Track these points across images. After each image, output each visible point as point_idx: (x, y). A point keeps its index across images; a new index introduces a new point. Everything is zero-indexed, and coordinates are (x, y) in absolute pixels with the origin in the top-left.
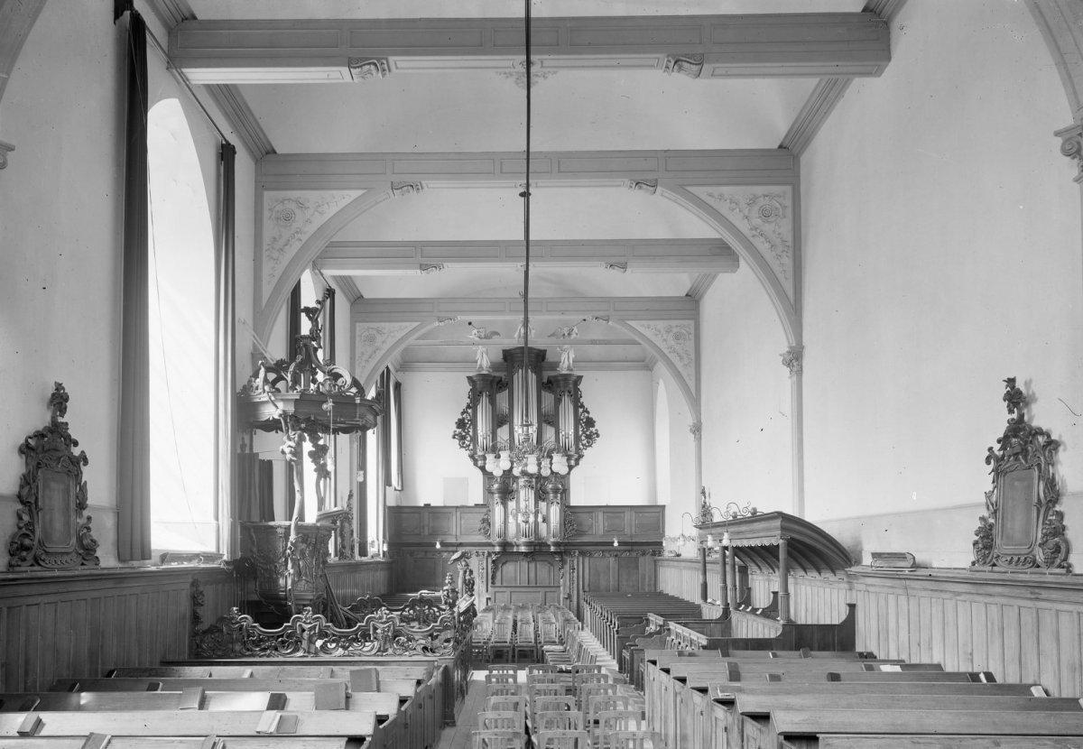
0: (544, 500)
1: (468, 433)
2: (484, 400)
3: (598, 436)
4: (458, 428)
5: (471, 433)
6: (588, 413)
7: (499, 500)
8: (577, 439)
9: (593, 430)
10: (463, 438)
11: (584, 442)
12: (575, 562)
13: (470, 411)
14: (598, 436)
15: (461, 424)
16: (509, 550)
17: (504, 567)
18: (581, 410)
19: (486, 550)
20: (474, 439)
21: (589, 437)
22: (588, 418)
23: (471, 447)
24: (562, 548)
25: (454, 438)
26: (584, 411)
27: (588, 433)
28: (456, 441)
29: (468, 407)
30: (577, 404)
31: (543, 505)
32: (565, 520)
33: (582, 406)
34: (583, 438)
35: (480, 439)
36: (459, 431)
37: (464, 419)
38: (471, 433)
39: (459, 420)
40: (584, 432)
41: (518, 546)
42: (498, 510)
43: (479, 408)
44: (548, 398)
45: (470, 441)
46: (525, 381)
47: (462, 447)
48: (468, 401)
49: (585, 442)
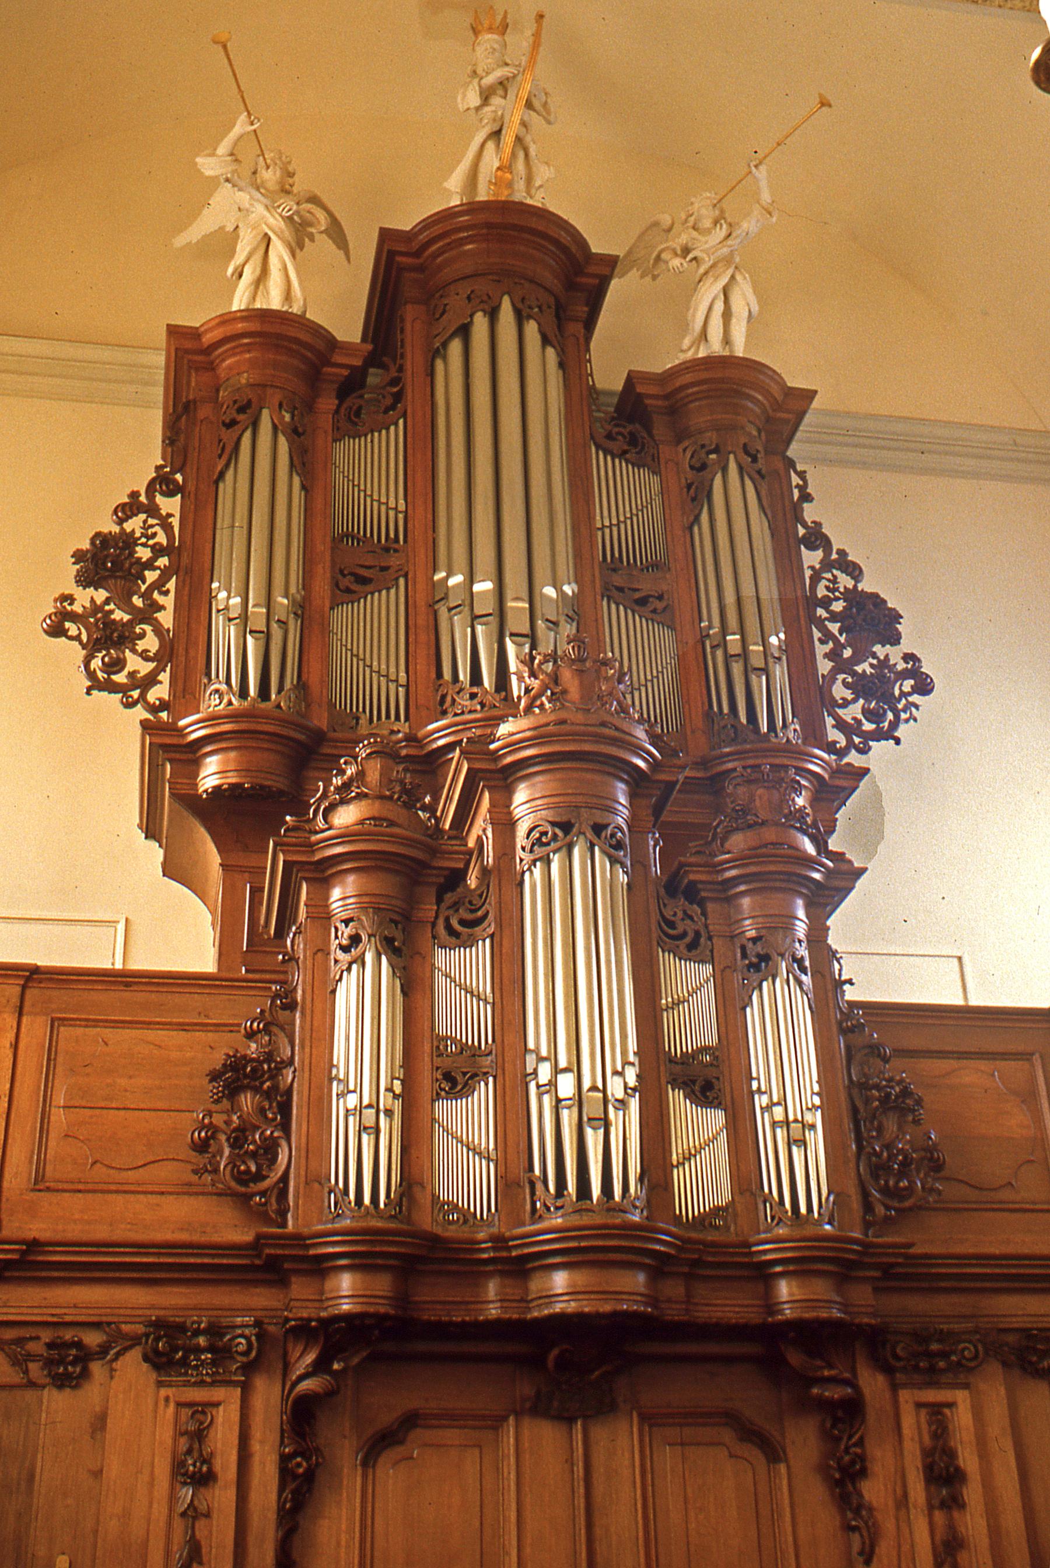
0: (692, 948)
1: (148, 614)
2: (266, 448)
3: (924, 687)
4: (85, 580)
5: (166, 618)
7: (366, 925)
8: (812, 699)
9: (894, 654)
10: (109, 638)
11: (848, 714)
12: (962, 1417)
13: (170, 505)
14: (924, 687)
15: (106, 561)
16: (437, 1301)
17: (390, 1476)
18: (811, 558)
19: (244, 1306)
20: (186, 654)
21: (876, 689)
22: (853, 596)
23: (160, 692)
24: (862, 1296)
25: (56, 630)
26: (827, 564)
27: (864, 667)
28: (70, 652)
29: (162, 483)
30: (790, 528)
31: (689, 981)
32: (859, 1087)
33: (817, 538)
35: (225, 635)
36: (84, 598)
37: (128, 541)
38: (166, 618)
39: (102, 541)
40: (841, 666)
41: (521, 1267)
42: (357, 1011)
43: (232, 489)
44: (628, 496)
45: (162, 658)
47: (96, 685)
49: (853, 712)
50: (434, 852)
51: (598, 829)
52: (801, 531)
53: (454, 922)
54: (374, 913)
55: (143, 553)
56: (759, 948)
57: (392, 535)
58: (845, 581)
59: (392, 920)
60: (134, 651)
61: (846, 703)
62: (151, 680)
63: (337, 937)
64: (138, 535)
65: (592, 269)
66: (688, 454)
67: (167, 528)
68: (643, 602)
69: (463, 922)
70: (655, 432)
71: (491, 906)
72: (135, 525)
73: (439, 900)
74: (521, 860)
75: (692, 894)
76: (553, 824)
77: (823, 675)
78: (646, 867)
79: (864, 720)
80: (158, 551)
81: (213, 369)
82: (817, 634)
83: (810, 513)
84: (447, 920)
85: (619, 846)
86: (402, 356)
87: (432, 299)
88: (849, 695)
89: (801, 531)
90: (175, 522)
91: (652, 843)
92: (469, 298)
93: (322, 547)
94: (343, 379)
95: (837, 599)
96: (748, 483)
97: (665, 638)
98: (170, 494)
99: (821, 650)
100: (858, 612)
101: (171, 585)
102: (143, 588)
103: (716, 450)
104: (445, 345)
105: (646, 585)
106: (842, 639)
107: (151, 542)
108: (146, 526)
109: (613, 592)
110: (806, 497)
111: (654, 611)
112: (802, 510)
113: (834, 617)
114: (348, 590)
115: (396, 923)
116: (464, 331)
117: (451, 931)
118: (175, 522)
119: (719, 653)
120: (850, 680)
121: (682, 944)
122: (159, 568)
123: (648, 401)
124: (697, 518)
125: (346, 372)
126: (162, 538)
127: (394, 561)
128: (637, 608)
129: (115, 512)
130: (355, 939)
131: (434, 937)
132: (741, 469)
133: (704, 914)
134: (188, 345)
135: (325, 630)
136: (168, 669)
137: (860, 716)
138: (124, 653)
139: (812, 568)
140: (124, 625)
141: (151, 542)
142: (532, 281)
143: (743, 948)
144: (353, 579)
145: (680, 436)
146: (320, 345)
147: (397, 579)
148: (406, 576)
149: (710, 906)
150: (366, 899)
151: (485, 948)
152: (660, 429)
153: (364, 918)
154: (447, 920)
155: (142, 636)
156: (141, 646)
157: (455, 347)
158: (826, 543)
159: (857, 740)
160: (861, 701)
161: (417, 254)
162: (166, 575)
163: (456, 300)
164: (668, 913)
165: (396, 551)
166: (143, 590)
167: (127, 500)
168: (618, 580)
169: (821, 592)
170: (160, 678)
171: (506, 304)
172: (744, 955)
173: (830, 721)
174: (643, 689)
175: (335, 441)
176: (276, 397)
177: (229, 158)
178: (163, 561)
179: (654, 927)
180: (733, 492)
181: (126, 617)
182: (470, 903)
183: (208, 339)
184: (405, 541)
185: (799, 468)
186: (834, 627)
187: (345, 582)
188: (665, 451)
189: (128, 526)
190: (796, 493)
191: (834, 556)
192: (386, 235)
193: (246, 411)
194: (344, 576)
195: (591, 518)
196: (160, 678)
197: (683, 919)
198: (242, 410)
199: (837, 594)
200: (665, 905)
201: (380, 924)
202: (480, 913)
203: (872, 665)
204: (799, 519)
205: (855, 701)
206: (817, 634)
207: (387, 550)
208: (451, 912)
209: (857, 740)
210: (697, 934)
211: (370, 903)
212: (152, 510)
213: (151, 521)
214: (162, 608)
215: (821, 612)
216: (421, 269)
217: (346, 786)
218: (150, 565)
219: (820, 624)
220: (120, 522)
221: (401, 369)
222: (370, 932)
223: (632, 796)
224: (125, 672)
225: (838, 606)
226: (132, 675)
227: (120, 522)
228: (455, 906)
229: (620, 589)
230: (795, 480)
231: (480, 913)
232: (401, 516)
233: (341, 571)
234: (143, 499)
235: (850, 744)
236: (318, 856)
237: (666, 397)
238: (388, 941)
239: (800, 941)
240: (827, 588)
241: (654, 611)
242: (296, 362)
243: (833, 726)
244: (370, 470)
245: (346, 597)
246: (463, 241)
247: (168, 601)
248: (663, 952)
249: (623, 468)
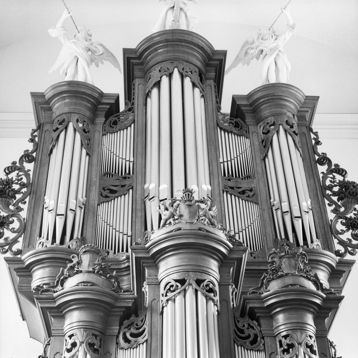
6: (342, 172)
13: (29, 166)
18: (322, 169)
26: (330, 171)
29: (27, 157)
33: (324, 160)
34: (339, 227)
37: (9, 183)
38: (24, 214)
40: (339, 216)
44: (235, 149)
46: (176, 106)
48: (30, 147)
49: (347, 236)
50: (117, 299)
51: (199, 282)
52: (317, 157)
53: (128, 335)
54: (85, 331)
55: (16, 187)
56: (288, 341)
57: (127, 172)
58: (339, 178)
59: (93, 334)
60: (8, 228)
61: (343, 232)
62: (15, 241)
63: (66, 345)
64: (14, 179)
65: (216, 57)
66: (262, 128)
67: (27, 175)
68: (243, 192)
69: (132, 335)
70: (246, 121)
71: (146, 326)
72: (13, 175)
73: (121, 324)
74: (162, 301)
75: (252, 315)
76: (176, 281)
77: (331, 220)
78: (228, 302)
79: (352, 240)
80: (23, 185)
81: (51, 110)
82: (327, 202)
83: (320, 149)
84: (124, 334)
85: (211, 290)
86: (133, 99)
87: (145, 75)
88: (344, 228)
89: (317, 157)
90: (31, 173)
91: (231, 290)
92: (160, 71)
93: (95, 178)
94: (107, 110)
95: (336, 186)
96: (290, 138)
97: (254, 209)
98: (30, 162)
99: (329, 209)
100: (346, 190)
101: (27, 200)
102: (15, 201)
103: (274, 124)
104: (150, 92)
105: (245, 185)
106: (339, 203)
107: (19, 182)
108: (18, 175)
109: (229, 190)
110: (318, 143)
111: (248, 196)
112: (317, 148)
113: (335, 194)
114: (107, 197)
115: (96, 336)
116: (158, 84)
117: (127, 340)
118: (31, 173)
119: (279, 212)
120: (344, 221)
121: (248, 341)
122: (22, 193)
123: (243, 108)
124: (266, 156)
125: (108, 107)
126: (25, 180)
127: (127, 182)
128: (240, 195)
129: (5, 170)
130: (74, 345)
131: (117, 343)
132: (286, 131)
133: (259, 325)
134: (40, 100)
135: (96, 215)
136: (23, 236)
137: (350, 238)
138: (3, 230)
139: (323, 173)
140: (4, 218)
141: (19, 182)
142: (187, 62)
143: (280, 342)
144: (108, 191)
145: (258, 121)
146: (96, 95)
147: (129, 190)
148: (132, 188)
149: (262, 321)
150: (81, 324)
151: (143, 348)
152: (249, 120)
153: (78, 334)
154: (124, 334)
155: (12, 222)
156: (11, 226)
157: (155, 91)
158: (329, 162)
159: (350, 249)
160: (351, 231)
161: (140, 57)
162: (25, 195)
163: (155, 74)
164: (240, 325)
165: (129, 178)
166: (14, 202)
167: (10, 165)
168: (231, 184)
169: (328, 183)
170: (18, 240)
171: (176, 71)
172: (281, 346)
173: (336, 241)
174: (244, 232)
175: (103, 135)
176: (75, 117)
177: (62, 29)
178: (24, 190)
179: (232, 332)
180: (282, 142)
181: (5, 214)
182: (137, 325)
183: (48, 96)
184: (133, 173)
185: (314, 131)
186: (335, 198)
187: (105, 193)
188: (252, 128)
189: (10, 176)
190: (313, 142)
191: (333, 167)
192: (126, 51)
193: (64, 124)
194: (105, 190)
195: (217, 158)
196: (18, 240)
197: (248, 328)
198: (60, 124)
199: (335, 183)
200: (238, 321)
201: (87, 336)
202: (141, 330)
203: (355, 214)
204: (315, 152)
205: (348, 230)
206: (327, 202)
207: (125, 178)
208: (126, 330)
209: (350, 249)
210: (256, 336)
211: (86, 327)
212: (21, 169)
213: (20, 173)
214: (22, 209)
215: (328, 192)
216: (142, 64)
217: (72, 268)
218: (18, 192)
219: (328, 197)
220: (7, 174)
221: (133, 104)
222: (81, 341)
223: (221, 268)
224: (3, 238)
225: (336, 189)
226: (6, 239)
227: (7, 174)
228: (129, 327)
229: (232, 188)
230: (313, 136)
231: (141, 330)
232: (131, 164)
233: (104, 189)
234: (18, 164)
235: (346, 251)
236: (58, 303)
237: (251, 105)
238: (91, 345)
239: (311, 337)
240: (331, 181)
241: (248, 196)
242: (89, 105)
243: (338, 243)
244: (118, 146)
245: (105, 199)
246: (156, 50)
247: (25, 207)
248: (238, 346)
249: (232, 137)
